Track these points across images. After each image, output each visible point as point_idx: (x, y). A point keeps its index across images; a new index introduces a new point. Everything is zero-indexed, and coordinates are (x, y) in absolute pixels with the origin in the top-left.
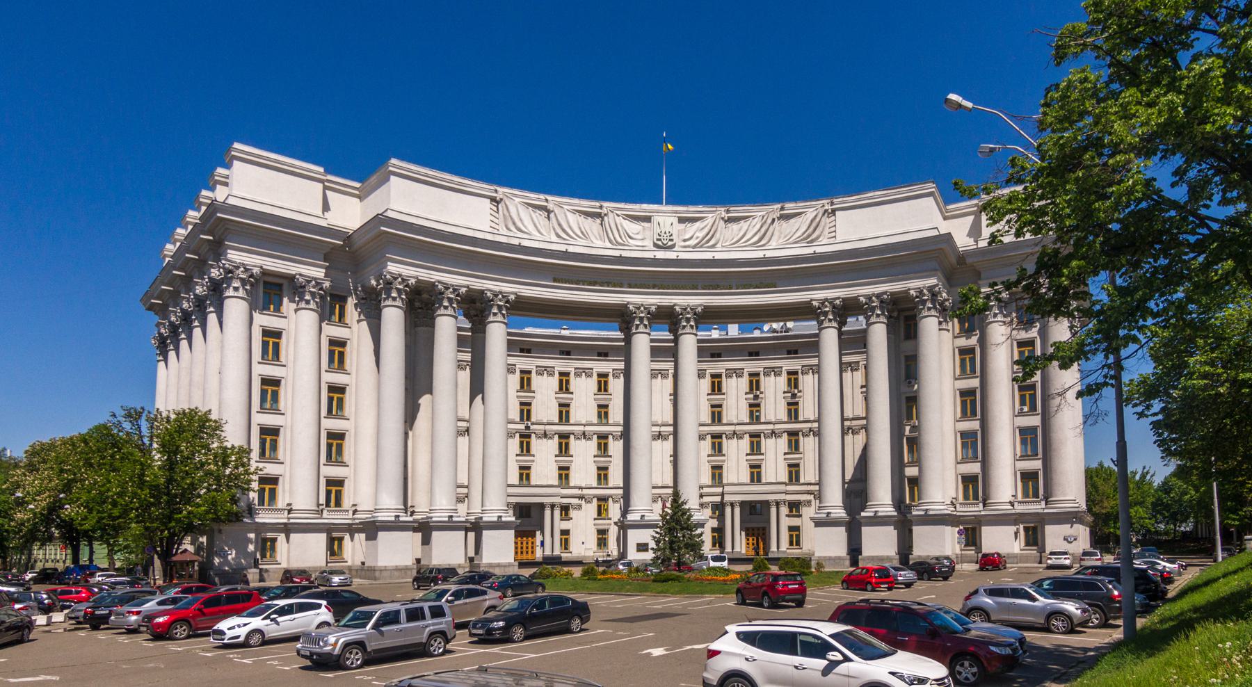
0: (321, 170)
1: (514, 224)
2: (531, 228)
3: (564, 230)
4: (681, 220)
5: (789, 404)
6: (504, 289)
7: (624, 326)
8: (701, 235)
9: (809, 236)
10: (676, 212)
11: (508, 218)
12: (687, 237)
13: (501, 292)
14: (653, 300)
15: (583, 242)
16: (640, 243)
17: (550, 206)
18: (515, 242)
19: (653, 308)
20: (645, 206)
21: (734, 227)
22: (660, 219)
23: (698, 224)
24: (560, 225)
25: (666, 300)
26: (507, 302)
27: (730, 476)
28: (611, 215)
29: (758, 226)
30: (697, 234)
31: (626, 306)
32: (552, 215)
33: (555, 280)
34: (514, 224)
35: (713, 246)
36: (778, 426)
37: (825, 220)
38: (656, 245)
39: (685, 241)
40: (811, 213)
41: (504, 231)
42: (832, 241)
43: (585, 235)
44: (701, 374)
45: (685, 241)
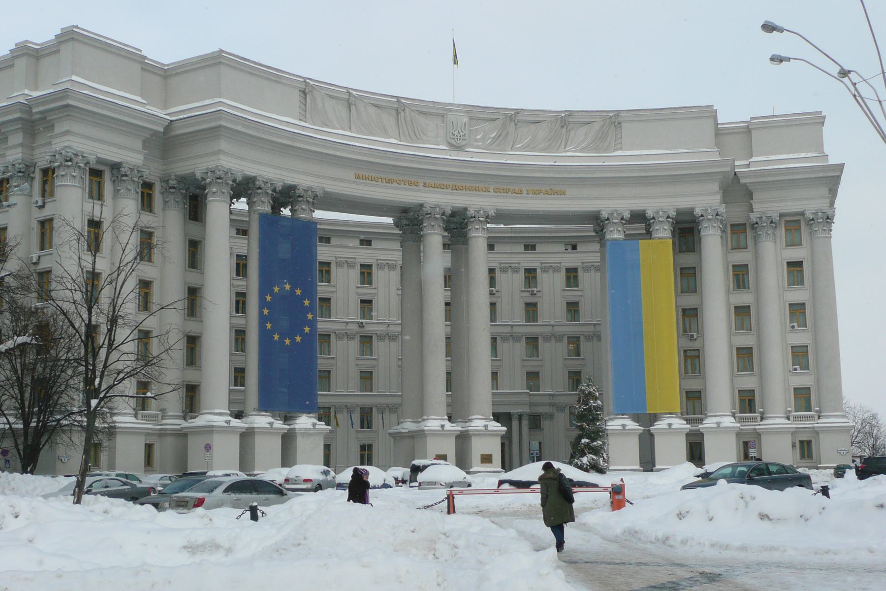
5: (527, 304)
6: (313, 184)
7: (405, 222)
10: (467, 112)
13: (311, 188)
26: (316, 197)
28: (407, 110)
32: (353, 108)
33: (357, 177)
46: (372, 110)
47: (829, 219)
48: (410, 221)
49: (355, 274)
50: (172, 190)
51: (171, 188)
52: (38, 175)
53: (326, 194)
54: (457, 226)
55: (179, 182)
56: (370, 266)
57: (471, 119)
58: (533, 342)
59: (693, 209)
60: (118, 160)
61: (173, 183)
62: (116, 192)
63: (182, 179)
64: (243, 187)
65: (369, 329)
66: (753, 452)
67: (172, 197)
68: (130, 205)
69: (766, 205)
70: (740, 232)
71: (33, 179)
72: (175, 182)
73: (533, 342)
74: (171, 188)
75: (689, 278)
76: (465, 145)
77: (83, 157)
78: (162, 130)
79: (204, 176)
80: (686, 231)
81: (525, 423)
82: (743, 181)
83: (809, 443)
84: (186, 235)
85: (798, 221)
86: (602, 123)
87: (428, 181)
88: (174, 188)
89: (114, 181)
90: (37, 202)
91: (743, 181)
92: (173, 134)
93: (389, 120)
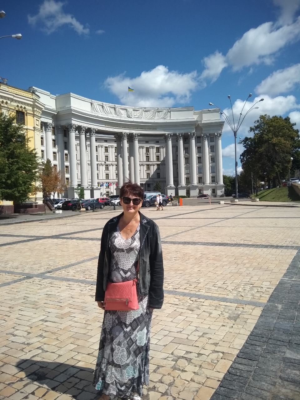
0: (49, 93)
1: (96, 110)
2: (99, 111)
3: (106, 112)
4: (134, 110)
5: (146, 157)
12: (135, 115)
14: (128, 131)
15: (111, 115)
18: (97, 115)
23: (138, 112)
24: (105, 110)
26: (96, 131)
27: (111, 177)
31: (122, 133)
34: (96, 110)
35: (142, 118)
36: (144, 163)
38: (127, 116)
39: (135, 116)
41: (94, 112)
45: (135, 116)
46: (108, 108)
47: (220, 135)
48: (119, 137)
49: (103, 149)
53: (98, 130)
54: (131, 138)
56: (107, 147)
58: (148, 165)
59: (188, 134)
60: (46, 122)
61: (60, 127)
62: (45, 130)
63: (62, 126)
64: (79, 129)
65: (107, 163)
66: (202, 192)
69: (206, 132)
70: (199, 139)
73: (148, 165)
75: (187, 150)
76: (132, 117)
78: (56, 114)
80: (187, 139)
81: (147, 186)
82: (200, 126)
83: (215, 189)
91: (200, 126)
93: (113, 110)
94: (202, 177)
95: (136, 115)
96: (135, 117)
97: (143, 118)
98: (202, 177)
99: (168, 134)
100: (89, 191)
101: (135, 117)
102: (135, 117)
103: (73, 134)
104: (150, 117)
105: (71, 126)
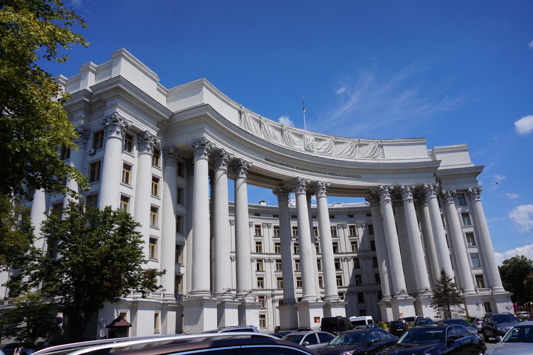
1: (248, 125)
8: (326, 147)
9: (373, 155)
11: (245, 121)
12: (319, 147)
13: (246, 161)
16: (298, 147)
17: (262, 120)
19: (309, 181)
20: (298, 129)
21: (339, 146)
22: (308, 137)
23: (323, 142)
25: (314, 178)
29: (349, 147)
30: (323, 147)
32: (262, 126)
34: (248, 125)
37: (379, 149)
40: (372, 145)
42: (383, 159)
43: (276, 138)
44: (250, 225)
45: (318, 149)
50: (171, 155)
51: (170, 154)
52: (92, 136)
55: (175, 151)
57: (315, 138)
61: (172, 151)
67: (170, 159)
68: (147, 158)
71: (88, 139)
72: (173, 150)
74: (170, 154)
77: (125, 122)
79: (194, 145)
84: (177, 184)
85: (463, 194)
86: (374, 145)
87: (298, 167)
88: (172, 154)
89: (139, 144)
90: (90, 151)
92: (174, 122)
94: (363, 293)
95: (321, 148)
96: (318, 152)
97: (333, 154)
98: (363, 293)
99: (384, 187)
100: (236, 311)
101: (319, 151)
102: (319, 151)
103: (202, 166)
104: (347, 154)
105: (202, 144)
